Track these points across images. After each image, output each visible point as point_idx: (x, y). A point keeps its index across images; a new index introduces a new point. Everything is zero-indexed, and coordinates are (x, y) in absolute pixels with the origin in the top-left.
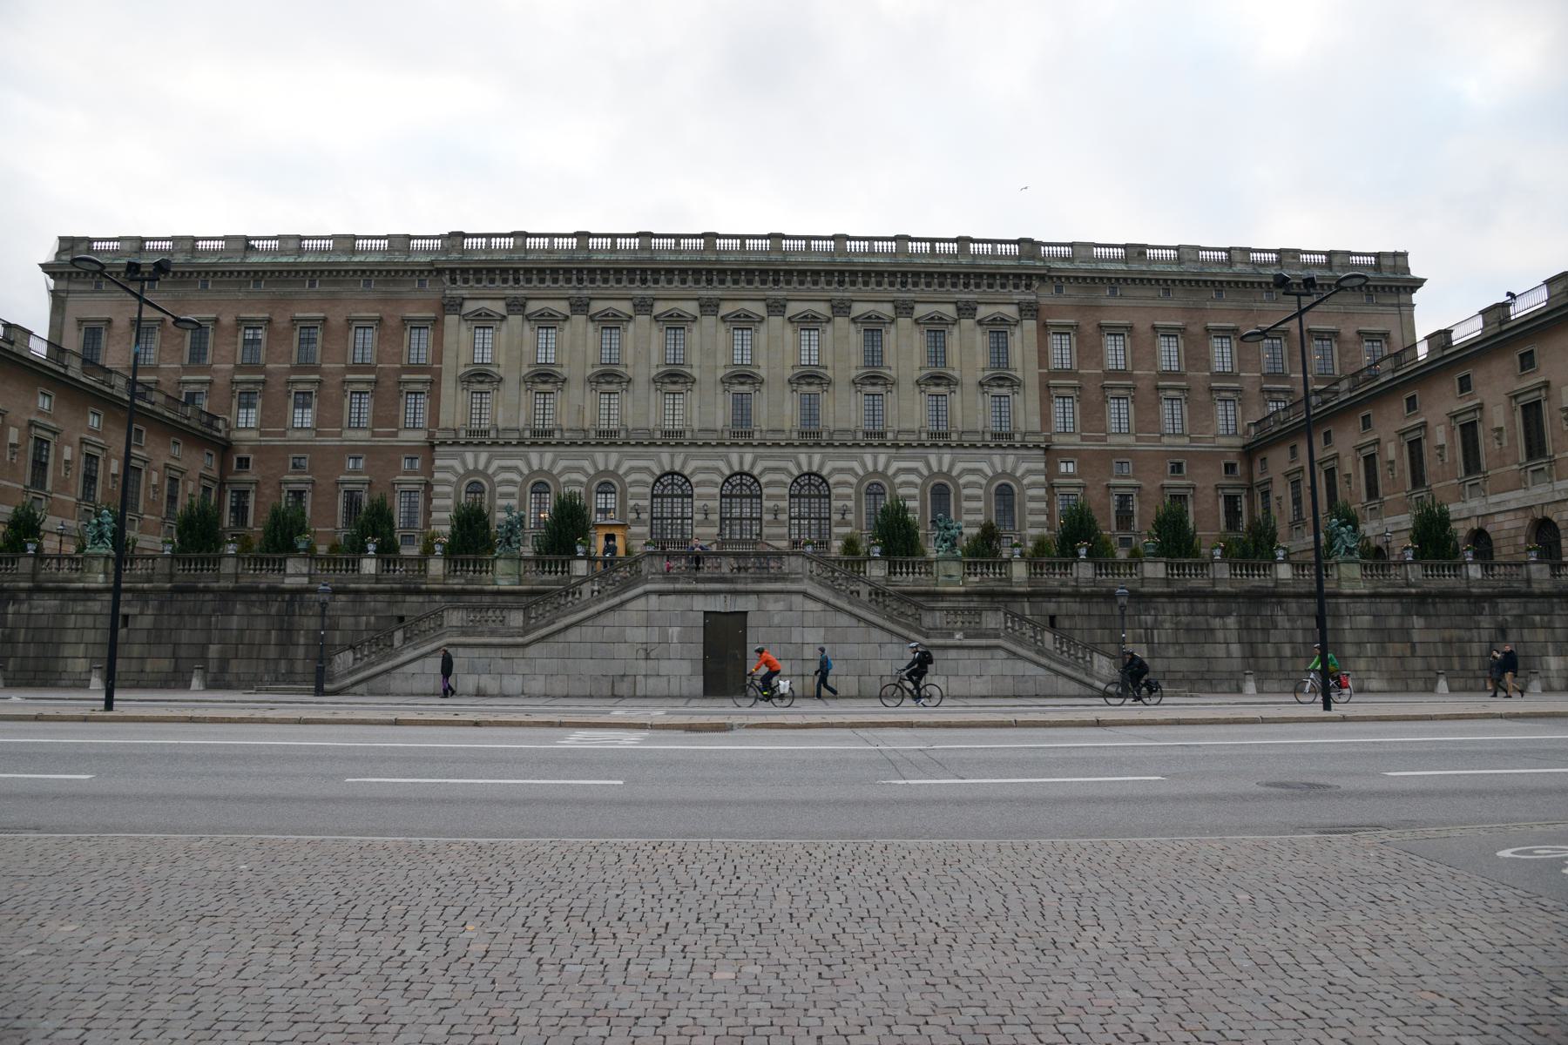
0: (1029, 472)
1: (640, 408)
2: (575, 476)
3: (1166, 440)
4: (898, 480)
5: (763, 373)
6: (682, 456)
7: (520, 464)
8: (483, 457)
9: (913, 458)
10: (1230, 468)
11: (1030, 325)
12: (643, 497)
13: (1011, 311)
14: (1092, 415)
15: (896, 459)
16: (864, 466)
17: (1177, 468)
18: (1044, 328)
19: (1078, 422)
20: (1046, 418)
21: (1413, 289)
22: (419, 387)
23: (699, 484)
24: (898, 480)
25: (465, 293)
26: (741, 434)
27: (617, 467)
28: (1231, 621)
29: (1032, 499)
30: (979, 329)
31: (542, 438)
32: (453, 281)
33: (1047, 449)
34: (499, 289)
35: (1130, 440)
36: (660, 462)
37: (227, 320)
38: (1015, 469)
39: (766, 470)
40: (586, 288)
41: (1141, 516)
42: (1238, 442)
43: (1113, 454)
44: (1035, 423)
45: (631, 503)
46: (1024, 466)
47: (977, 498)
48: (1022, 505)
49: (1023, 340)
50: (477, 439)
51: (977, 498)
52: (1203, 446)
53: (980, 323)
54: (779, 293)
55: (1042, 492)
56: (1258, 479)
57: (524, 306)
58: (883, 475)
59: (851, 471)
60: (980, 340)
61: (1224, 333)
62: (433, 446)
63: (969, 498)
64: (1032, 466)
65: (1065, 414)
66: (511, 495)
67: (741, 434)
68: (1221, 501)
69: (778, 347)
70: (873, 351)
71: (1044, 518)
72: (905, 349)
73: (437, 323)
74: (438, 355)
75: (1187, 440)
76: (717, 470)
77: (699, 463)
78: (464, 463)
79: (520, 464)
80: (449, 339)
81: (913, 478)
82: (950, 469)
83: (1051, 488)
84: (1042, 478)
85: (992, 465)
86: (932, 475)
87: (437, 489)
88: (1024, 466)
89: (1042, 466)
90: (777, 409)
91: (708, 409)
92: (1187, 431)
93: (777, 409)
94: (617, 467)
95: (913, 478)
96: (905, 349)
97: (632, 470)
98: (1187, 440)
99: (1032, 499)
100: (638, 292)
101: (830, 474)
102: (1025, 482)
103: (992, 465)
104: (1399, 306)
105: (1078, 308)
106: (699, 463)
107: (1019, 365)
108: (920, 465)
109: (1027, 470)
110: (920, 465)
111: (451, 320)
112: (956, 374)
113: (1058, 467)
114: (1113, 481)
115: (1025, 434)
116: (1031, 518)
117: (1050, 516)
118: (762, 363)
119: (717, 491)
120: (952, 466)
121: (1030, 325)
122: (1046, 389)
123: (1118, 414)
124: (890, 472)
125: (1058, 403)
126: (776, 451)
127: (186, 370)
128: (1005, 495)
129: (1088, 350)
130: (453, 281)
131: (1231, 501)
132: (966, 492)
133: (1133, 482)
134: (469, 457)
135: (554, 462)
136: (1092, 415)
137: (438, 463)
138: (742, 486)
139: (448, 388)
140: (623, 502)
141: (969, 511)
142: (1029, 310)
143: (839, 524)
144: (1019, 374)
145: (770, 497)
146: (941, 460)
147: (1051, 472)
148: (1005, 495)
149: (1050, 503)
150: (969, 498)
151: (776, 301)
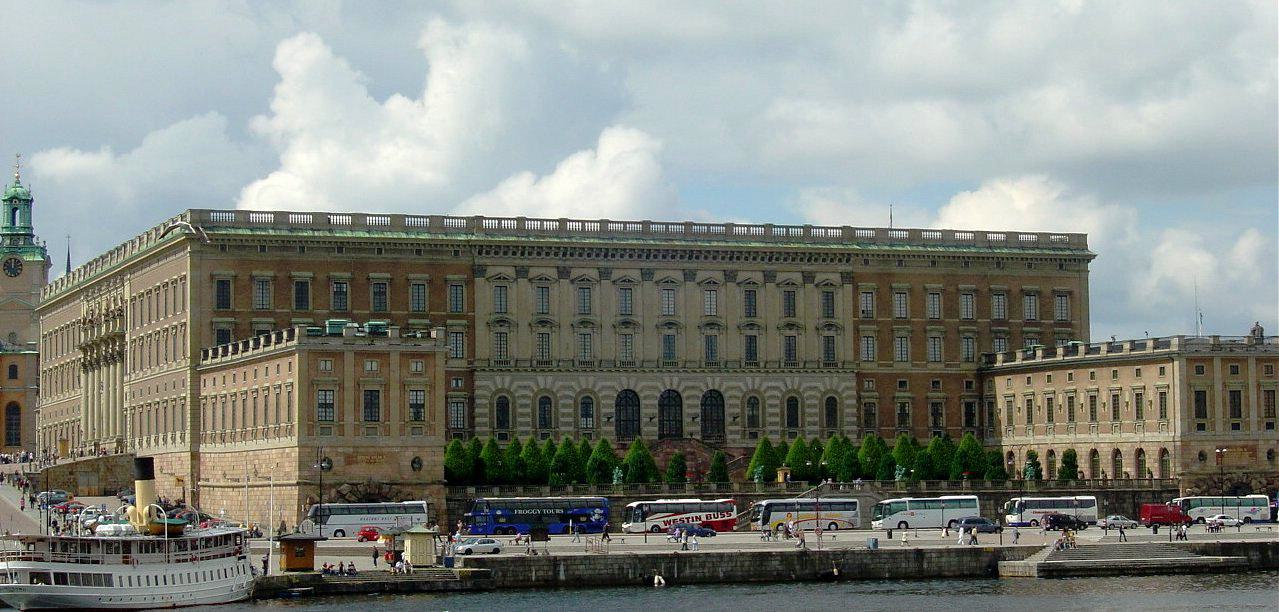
0: (848, 388)
1: (607, 345)
2: (567, 393)
3: (930, 366)
4: (767, 394)
5: (682, 321)
6: (634, 379)
7: (532, 384)
8: (508, 379)
9: (776, 380)
10: (969, 384)
11: (849, 287)
12: (610, 406)
13: (835, 278)
14: (885, 350)
15: (765, 380)
16: (746, 385)
17: (936, 383)
18: (856, 289)
19: (876, 354)
20: (857, 352)
21: (1089, 261)
22: (460, 329)
23: (645, 398)
24: (767, 394)
25: (488, 262)
26: (669, 361)
27: (594, 386)
28: (992, 502)
29: (848, 406)
30: (816, 290)
31: (544, 364)
32: (480, 253)
33: (857, 374)
34: (510, 260)
35: (908, 366)
36: (621, 384)
37: (321, 277)
38: (838, 386)
39: (687, 388)
40: (568, 259)
41: (914, 417)
42: (973, 366)
43: (898, 375)
44: (850, 356)
45: (603, 411)
46: (844, 385)
47: (815, 406)
48: (842, 411)
49: (843, 298)
50: (503, 364)
51: (815, 406)
52: (952, 371)
53: (817, 286)
54: (692, 265)
55: (854, 402)
56: (986, 393)
57: (527, 272)
58: (757, 391)
59: (738, 388)
60: (817, 297)
61: (967, 293)
62: (473, 371)
63: (809, 406)
64: (848, 384)
65: (869, 348)
66: (526, 406)
67: (669, 361)
68: (963, 406)
69: (693, 303)
70: (751, 309)
71: (855, 419)
72: (771, 303)
73: (470, 283)
74: (472, 305)
75: (942, 366)
76: (656, 388)
77: (644, 383)
78: (495, 383)
79: (532, 384)
80: (478, 295)
81: (776, 393)
82: (799, 388)
83: (859, 398)
84: (855, 393)
85: (824, 384)
86: (789, 391)
87: (478, 401)
88: (844, 385)
89: (854, 384)
90: (691, 346)
91: (648, 346)
92: (943, 360)
93: (691, 346)
94: (594, 386)
95: (776, 393)
96: (771, 303)
97: (603, 388)
98: (942, 366)
99: (848, 406)
100: (602, 263)
101: (726, 390)
102: (844, 395)
103: (824, 384)
104: (1078, 271)
105: (880, 276)
106: (644, 383)
107: (840, 316)
108: (780, 384)
109: (844, 386)
110: (780, 384)
111: (479, 281)
112: (802, 322)
113: (863, 386)
114: (897, 394)
115: (844, 363)
116: (848, 419)
117: (859, 418)
118: (681, 313)
119: (656, 402)
120: (800, 384)
121: (849, 287)
122: (857, 331)
123: (901, 349)
124: (762, 389)
125: (864, 342)
126: (694, 375)
127: (295, 315)
128: (831, 405)
129: (885, 306)
130: (480, 253)
131: (969, 406)
132: (808, 402)
133: (909, 395)
134: (498, 379)
135: (553, 383)
136: (885, 350)
137: (477, 383)
138: (671, 401)
139: (481, 330)
140: (598, 410)
141: (810, 415)
142: (847, 277)
143: (731, 424)
144: (840, 322)
145: (690, 406)
146: (793, 381)
147: (860, 387)
148: (831, 405)
149: (859, 409)
150: (809, 406)
151: (690, 270)
